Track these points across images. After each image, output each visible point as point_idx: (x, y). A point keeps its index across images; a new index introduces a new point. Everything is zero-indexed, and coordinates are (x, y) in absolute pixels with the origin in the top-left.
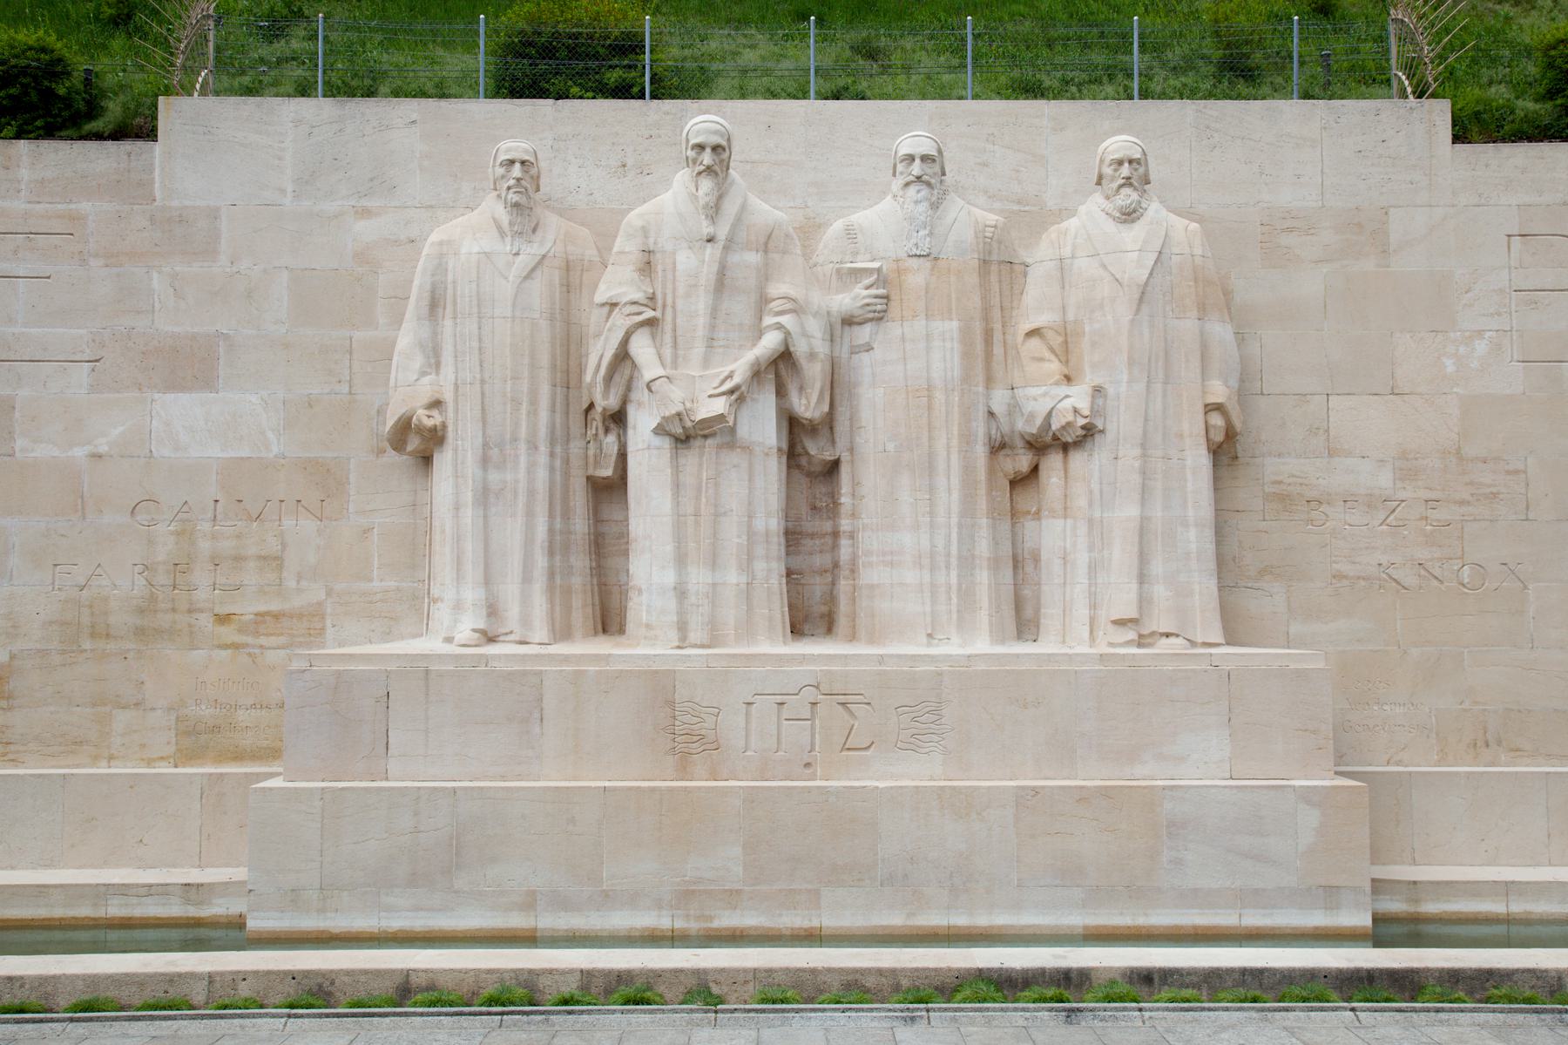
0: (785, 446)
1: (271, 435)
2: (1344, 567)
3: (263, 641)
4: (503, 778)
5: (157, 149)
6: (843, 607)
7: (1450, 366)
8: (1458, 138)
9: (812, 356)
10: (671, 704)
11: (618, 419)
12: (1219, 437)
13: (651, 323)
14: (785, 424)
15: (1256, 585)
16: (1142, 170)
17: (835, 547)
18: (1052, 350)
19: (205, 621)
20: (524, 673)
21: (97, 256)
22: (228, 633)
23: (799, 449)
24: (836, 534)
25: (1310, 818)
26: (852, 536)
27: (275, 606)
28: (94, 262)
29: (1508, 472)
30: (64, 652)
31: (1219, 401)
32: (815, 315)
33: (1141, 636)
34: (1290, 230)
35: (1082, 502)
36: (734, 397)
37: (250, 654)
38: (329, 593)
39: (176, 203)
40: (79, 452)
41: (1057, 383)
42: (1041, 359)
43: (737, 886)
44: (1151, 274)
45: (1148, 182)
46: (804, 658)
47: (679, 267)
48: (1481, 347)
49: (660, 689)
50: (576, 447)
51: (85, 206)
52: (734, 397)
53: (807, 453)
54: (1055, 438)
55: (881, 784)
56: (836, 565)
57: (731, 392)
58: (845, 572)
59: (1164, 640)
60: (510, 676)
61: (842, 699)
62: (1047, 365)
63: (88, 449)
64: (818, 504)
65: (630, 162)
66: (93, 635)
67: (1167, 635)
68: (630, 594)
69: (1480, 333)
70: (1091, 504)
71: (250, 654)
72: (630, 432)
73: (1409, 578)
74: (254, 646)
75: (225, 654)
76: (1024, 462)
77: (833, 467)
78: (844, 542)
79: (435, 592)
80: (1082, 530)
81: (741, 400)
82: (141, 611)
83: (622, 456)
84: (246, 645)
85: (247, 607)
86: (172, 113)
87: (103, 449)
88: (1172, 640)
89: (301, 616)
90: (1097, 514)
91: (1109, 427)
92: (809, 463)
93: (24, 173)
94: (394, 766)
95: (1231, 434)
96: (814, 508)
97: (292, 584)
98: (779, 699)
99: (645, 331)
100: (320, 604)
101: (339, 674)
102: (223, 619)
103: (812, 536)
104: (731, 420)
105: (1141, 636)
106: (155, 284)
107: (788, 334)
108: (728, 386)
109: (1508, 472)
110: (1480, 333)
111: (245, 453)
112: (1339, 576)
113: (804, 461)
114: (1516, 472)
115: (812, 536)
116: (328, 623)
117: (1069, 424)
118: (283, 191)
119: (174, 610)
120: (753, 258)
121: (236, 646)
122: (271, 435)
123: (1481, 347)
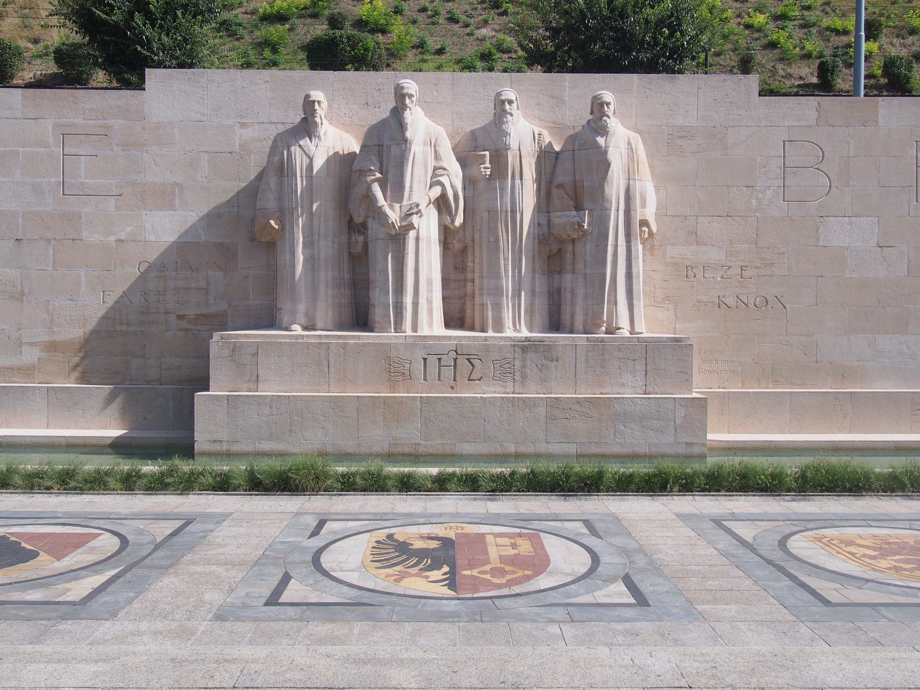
0: (442, 239)
1: (201, 232)
2: (703, 298)
3: (199, 327)
4: (311, 391)
7: (754, 204)
8: (760, 95)
10: (389, 358)
11: (364, 226)
12: (646, 236)
13: (377, 180)
14: (442, 228)
17: (465, 286)
18: (568, 195)
19: (173, 318)
20: (320, 343)
21: (117, 145)
22: (184, 324)
25: (681, 412)
26: (473, 281)
27: (204, 312)
28: (115, 148)
29: (779, 254)
30: (107, 332)
32: (457, 176)
34: (682, 137)
35: (580, 266)
38: (229, 306)
40: (112, 239)
43: (417, 441)
46: (450, 338)
47: (392, 153)
48: (769, 193)
49: (384, 352)
50: (344, 238)
51: (112, 122)
54: (568, 236)
55: (484, 396)
56: (466, 295)
61: (467, 357)
63: (116, 237)
65: (370, 101)
66: (121, 324)
69: (769, 187)
70: (585, 266)
72: (370, 231)
73: (731, 301)
75: (181, 333)
76: (555, 248)
78: (469, 284)
79: (278, 305)
80: (581, 280)
82: (143, 313)
83: (366, 244)
84: (191, 330)
85: (191, 312)
86: (152, 76)
87: (122, 237)
88: (621, 330)
90: (588, 271)
94: (260, 386)
96: (456, 268)
97: (212, 301)
98: (438, 357)
100: (225, 311)
102: (181, 317)
103: (455, 281)
104: (416, 225)
107: (443, 185)
109: (779, 254)
110: (769, 187)
112: (699, 301)
114: (783, 253)
115: (455, 281)
121: (186, 330)
122: (201, 232)
123: (769, 193)
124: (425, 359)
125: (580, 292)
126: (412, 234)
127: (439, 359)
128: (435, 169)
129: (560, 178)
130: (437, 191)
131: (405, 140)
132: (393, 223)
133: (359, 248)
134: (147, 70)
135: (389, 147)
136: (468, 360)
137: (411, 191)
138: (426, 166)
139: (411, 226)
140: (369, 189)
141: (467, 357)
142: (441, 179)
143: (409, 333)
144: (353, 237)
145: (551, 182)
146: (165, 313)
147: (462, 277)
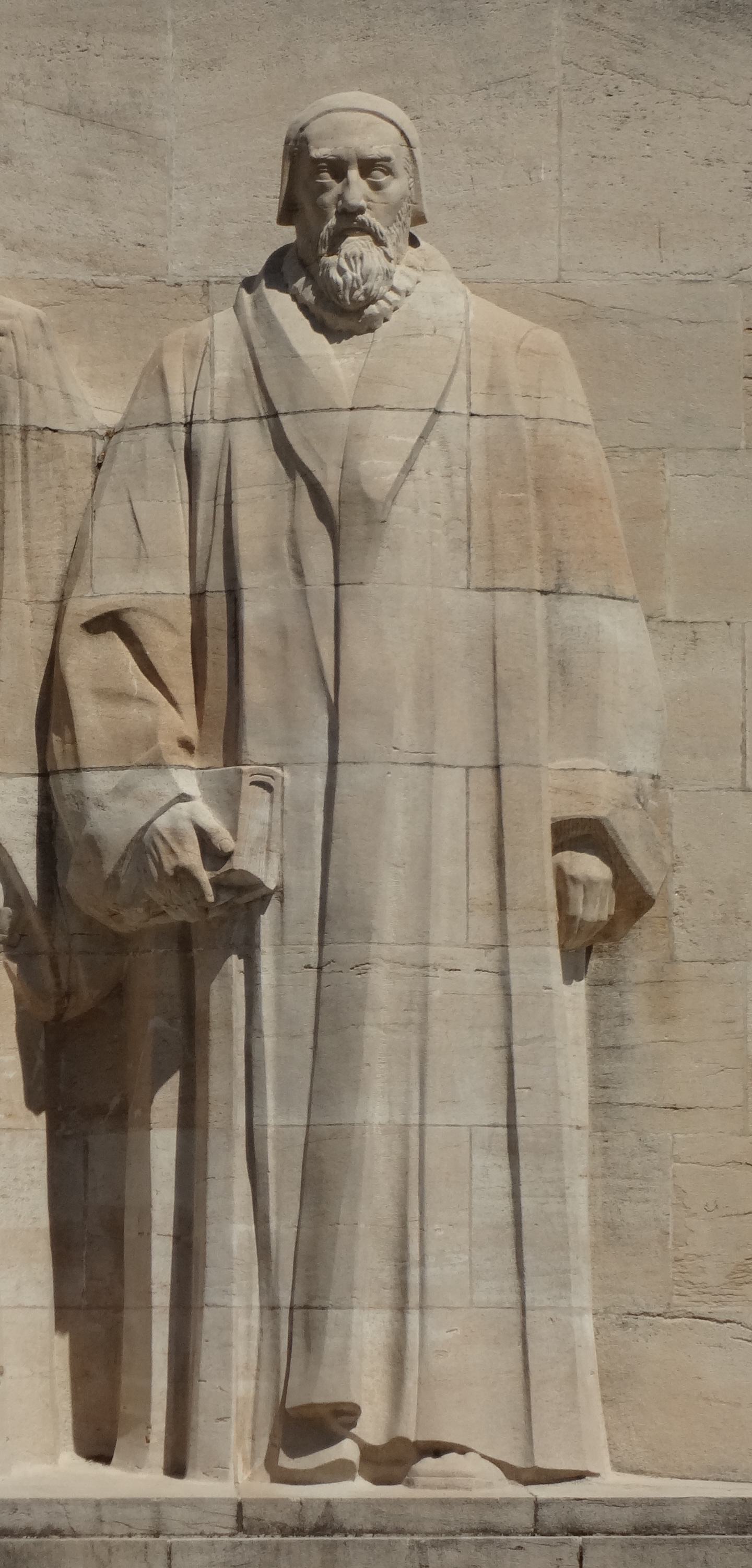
12: (597, 909)
15: (722, 1311)
16: (395, 187)
31: (599, 811)
33: (367, 1452)
41: (157, 764)
42: (122, 696)
44: (408, 469)
45: (419, 219)
59: (428, 1464)
62: (134, 711)
67: (437, 1450)
91: (291, 881)
95: (633, 899)
105: (367, 1452)
117: (184, 875)
125: (232, 1233)
129: (107, 589)
145: (61, 603)
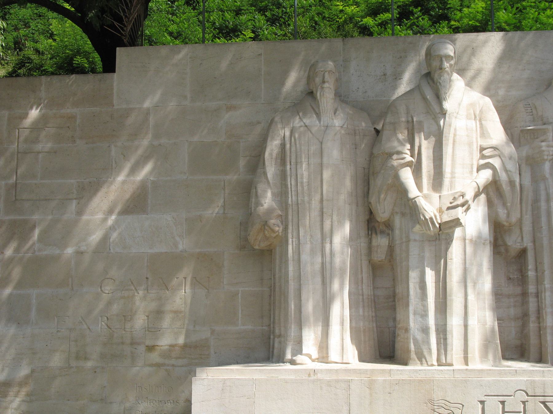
0: (492, 240)
1: (178, 239)
5: (115, 75)
6: (533, 340)
9: (511, 183)
10: (431, 401)
13: (409, 164)
19: (141, 349)
20: (337, 381)
23: (500, 242)
24: (524, 294)
26: (537, 295)
36: (465, 208)
37: (166, 370)
38: (213, 332)
39: (124, 106)
50: (363, 243)
52: (465, 208)
53: (505, 245)
56: (525, 315)
57: (463, 205)
58: (533, 317)
60: (329, 383)
61: (542, 399)
64: (511, 277)
66: (77, 358)
68: (397, 332)
71: (166, 370)
72: (397, 232)
74: (168, 365)
77: (523, 252)
79: (277, 331)
81: (468, 209)
84: (163, 365)
89: (196, 347)
92: (507, 251)
93: (43, 94)
98: (501, 399)
99: (408, 168)
101: (224, 381)
103: (509, 296)
106: (113, 153)
108: (460, 201)
111: (163, 251)
113: (502, 249)
115: (509, 296)
116: (212, 351)
118: (185, 97)
119: (123, 343)
120: (472, 124)
122: (178, 239)
124: (482, 402)
126: (458, 232)
127: (503, 403)
128: (482, 149)
130: (486, 175)
131: (443, 113)
132: (431, 219)
133: (380, 256)
134: (118, 48)
135: (420, 123)
136: (544, 403)
137: (453, 177)
138: (470, 144)
139: (457, 223)
140: (397, 177)
141: (542, 399)
142: (490, 160)
143: (458, 365)
144: (374, 243)
146: (132, 344)
147: (519, 290)
